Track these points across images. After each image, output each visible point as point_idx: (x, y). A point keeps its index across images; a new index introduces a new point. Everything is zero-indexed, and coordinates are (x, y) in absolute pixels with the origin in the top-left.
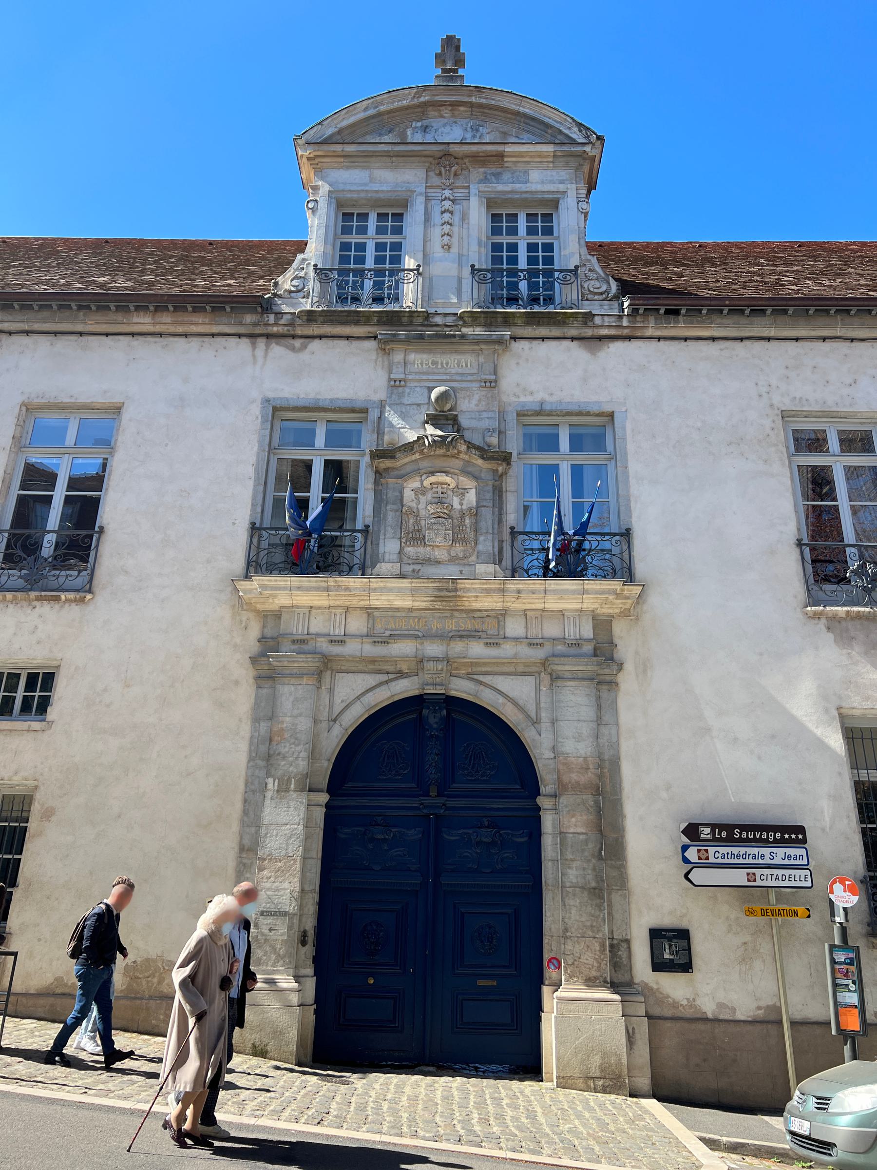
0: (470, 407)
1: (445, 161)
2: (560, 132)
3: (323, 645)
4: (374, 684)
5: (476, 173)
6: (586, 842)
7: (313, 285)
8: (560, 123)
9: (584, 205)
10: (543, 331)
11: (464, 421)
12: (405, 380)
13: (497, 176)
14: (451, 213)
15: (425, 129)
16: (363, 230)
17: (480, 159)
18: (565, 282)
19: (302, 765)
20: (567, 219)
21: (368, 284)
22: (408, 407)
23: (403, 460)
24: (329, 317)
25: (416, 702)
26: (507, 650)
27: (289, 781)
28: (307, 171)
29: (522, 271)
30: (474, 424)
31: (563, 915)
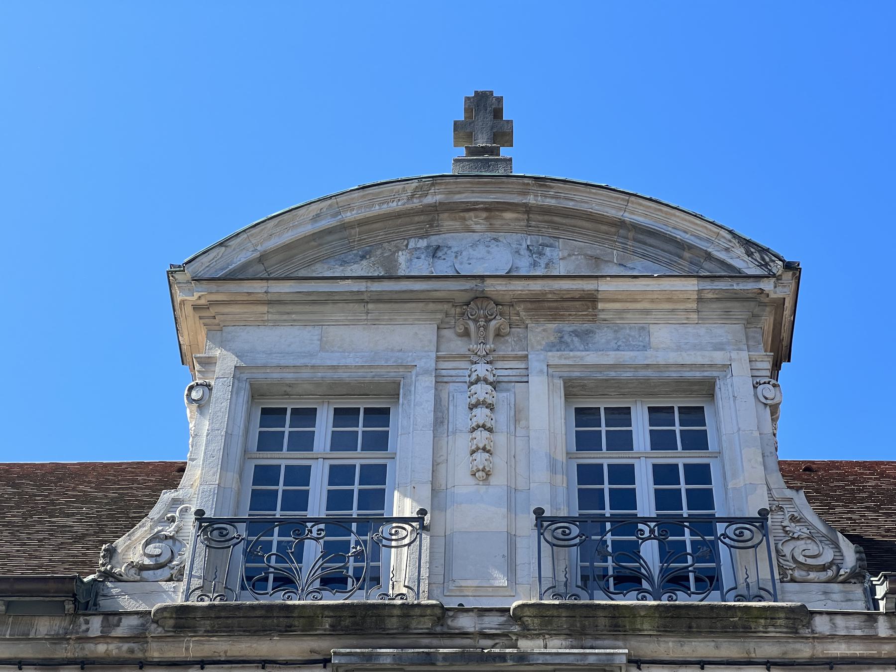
1: (475, 308)
2: (709, 256)
5: (540, 333)
7: (192, 552)
8: (708, 240)
9: (768, 391)
13: (584, 336)
14: (490, 407)
15: (435, 252)
16: (304, 442)
17: (547, 307)
18: (739, 543)
20: (734, 418)
21: (313, 550)
28: (194, 330)
29: (645, 520)
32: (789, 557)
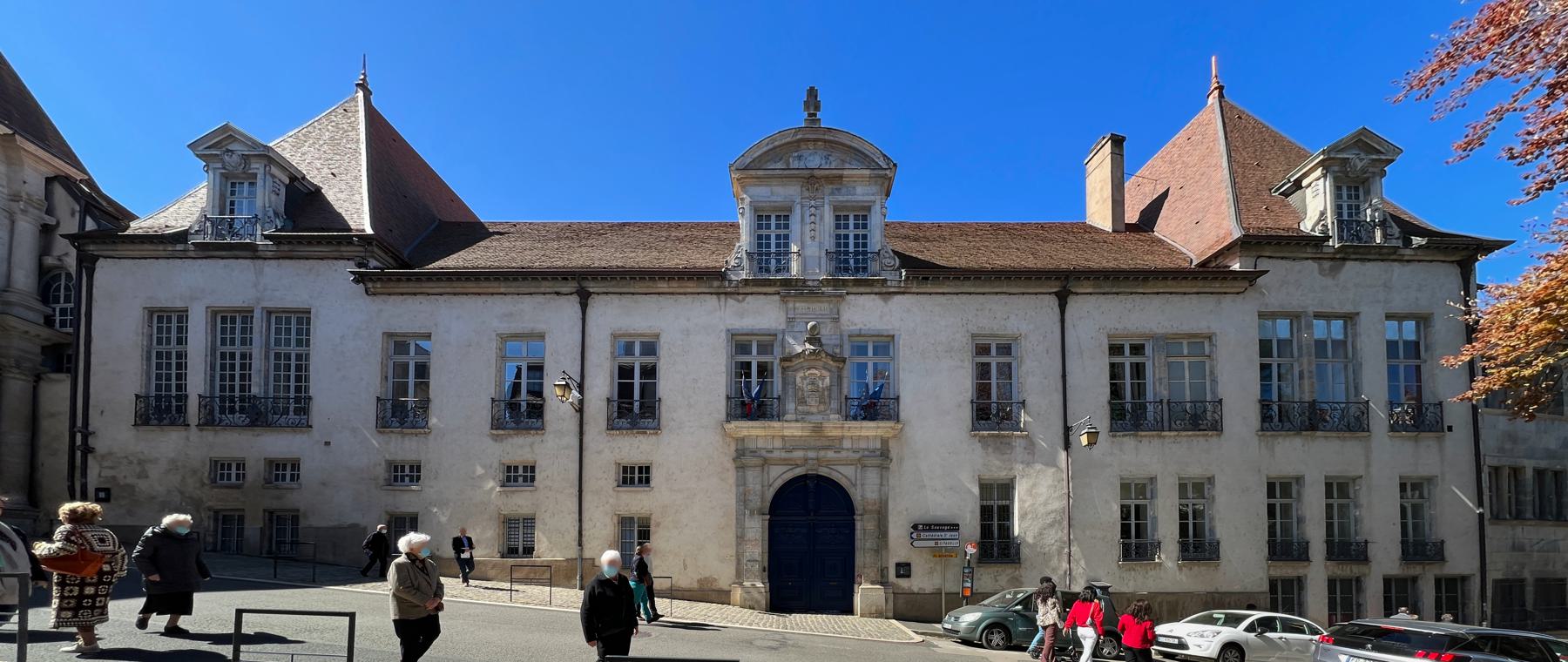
0: (826, 332)
1: (812, 180)
3: (764, 453)
5: (828, 188)
7: (745, 263)
10: (862, 290)
11: (824, 341)
15: (800, 157)
17: (830, 179)
18: (873, 260)
20: (875, 220)
21: (773, 262)
23: (796, 362)
24: (756, 282)
25: (804, 477)
26: (844, 454)
28: (737, 188)
31: (862, 559)
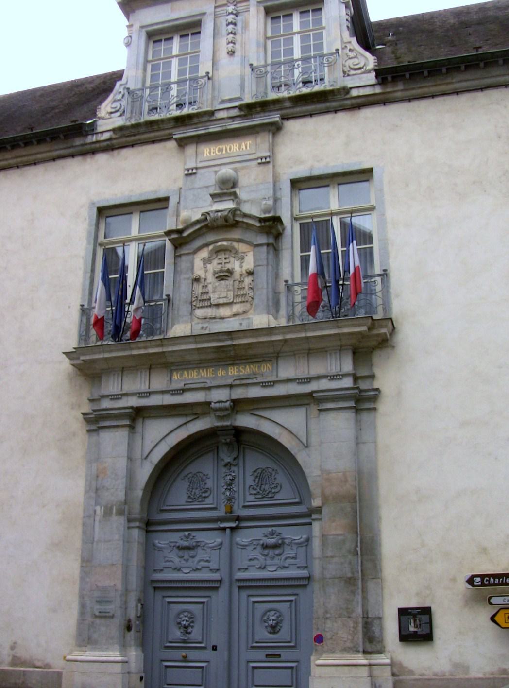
4: (175, 426)
6: (344, 542)
12: (196, 168)
14: (235, 24)
19: (121, 495)
22: (199, 190)
27: (111, 508)
29: (297, 60)
30: (253, 196)
32: (347, 67)
